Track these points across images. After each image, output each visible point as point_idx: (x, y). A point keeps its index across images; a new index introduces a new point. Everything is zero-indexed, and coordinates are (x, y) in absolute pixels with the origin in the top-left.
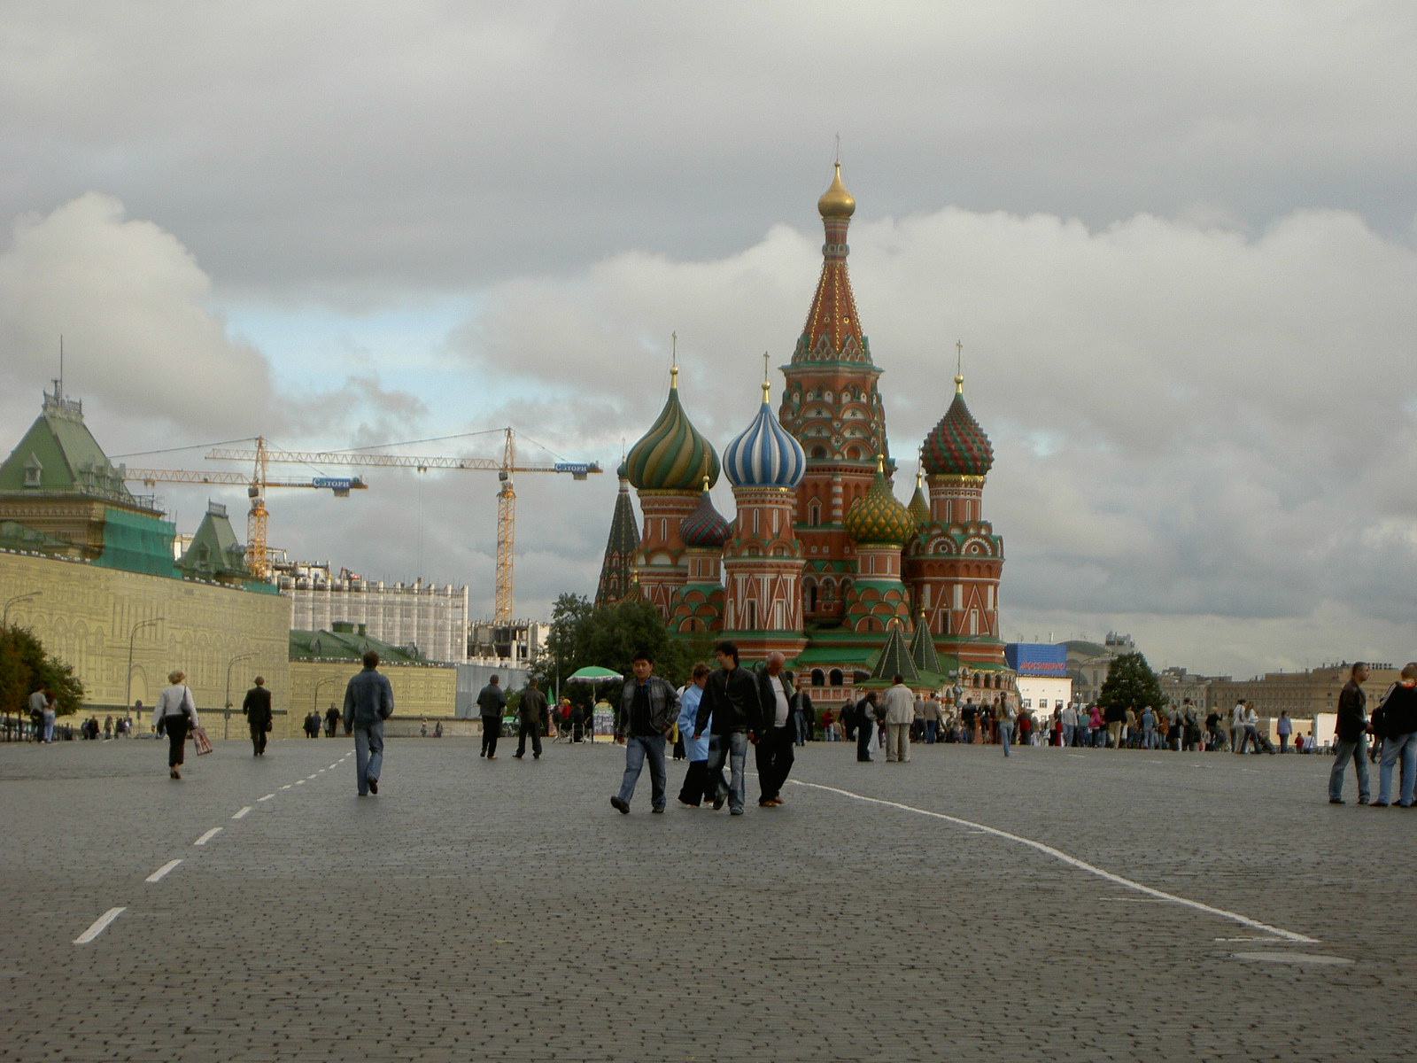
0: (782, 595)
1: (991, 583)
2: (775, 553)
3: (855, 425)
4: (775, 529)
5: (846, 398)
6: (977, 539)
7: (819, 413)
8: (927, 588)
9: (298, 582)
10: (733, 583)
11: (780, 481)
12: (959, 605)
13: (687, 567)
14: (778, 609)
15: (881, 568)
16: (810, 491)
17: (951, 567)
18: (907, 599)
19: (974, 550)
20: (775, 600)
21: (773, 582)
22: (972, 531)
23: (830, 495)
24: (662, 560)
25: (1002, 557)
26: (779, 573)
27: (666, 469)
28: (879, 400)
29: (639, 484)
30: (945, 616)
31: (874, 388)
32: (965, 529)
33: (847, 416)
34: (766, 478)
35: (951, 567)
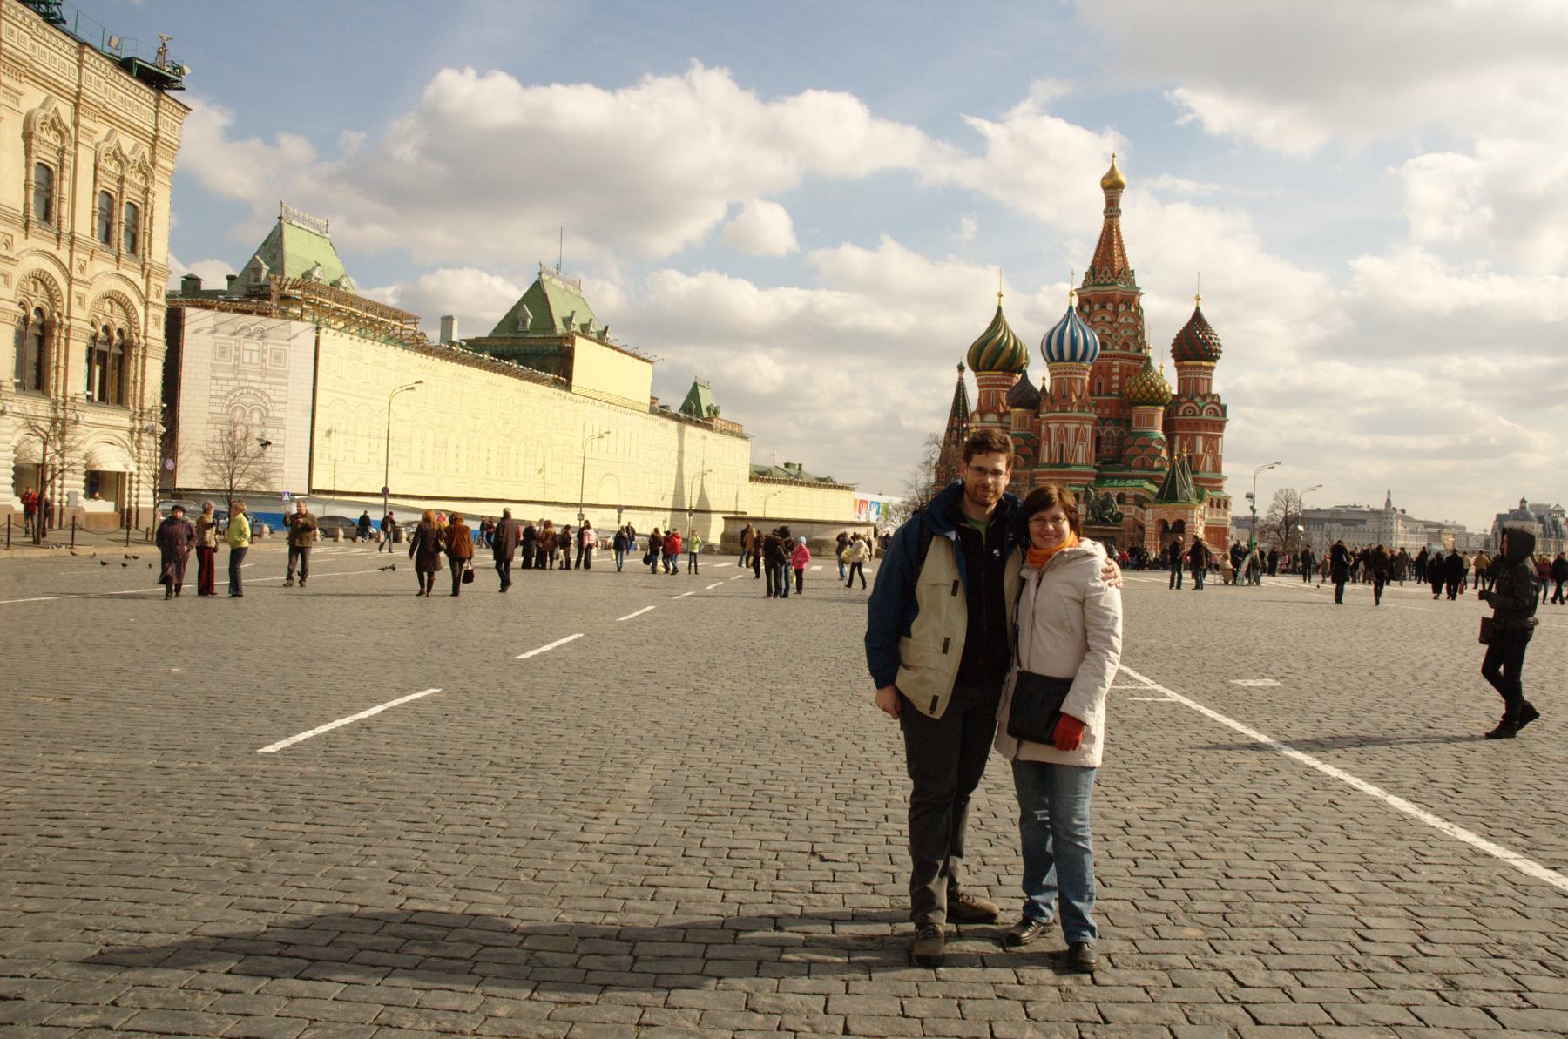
3: (1128, 325)
5: (1122, 308)
8: (1178, 439)
9: (673, 274)
10: (1049, 430)
11: (1083, 359)
12: (1200, 450)
14: (1080, 449)
17: (1197, 425)
21: (1077, 430)
23: (1110, 374)
27: (994, 355)
29: (976, 368)
33: (1122, 320)
34: (1073, 358)
35: (1197, 425)
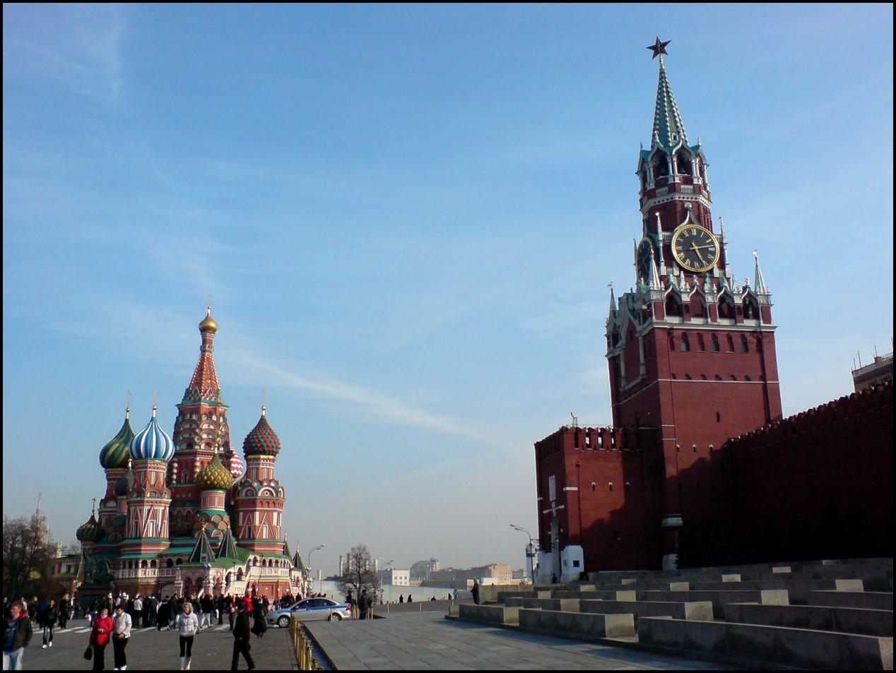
0: (155, 517)
1: (275, 511)
2: (150, 495)
4: (152, 483)
5: (204, 418)
6: (267, 488)
7: (191, 426)
8: (241, 514)
15: (212, 503)
16: (183, 465)
18: (227, 518)
19: (267, 493)
20: (149, 520)
21: (149, 510)
22: (265, 484)
25: (284, 498)
26: (152, 506)
28: (225, 420)
30: (250, 528)
31: (223, 415)
32: (261, 483)
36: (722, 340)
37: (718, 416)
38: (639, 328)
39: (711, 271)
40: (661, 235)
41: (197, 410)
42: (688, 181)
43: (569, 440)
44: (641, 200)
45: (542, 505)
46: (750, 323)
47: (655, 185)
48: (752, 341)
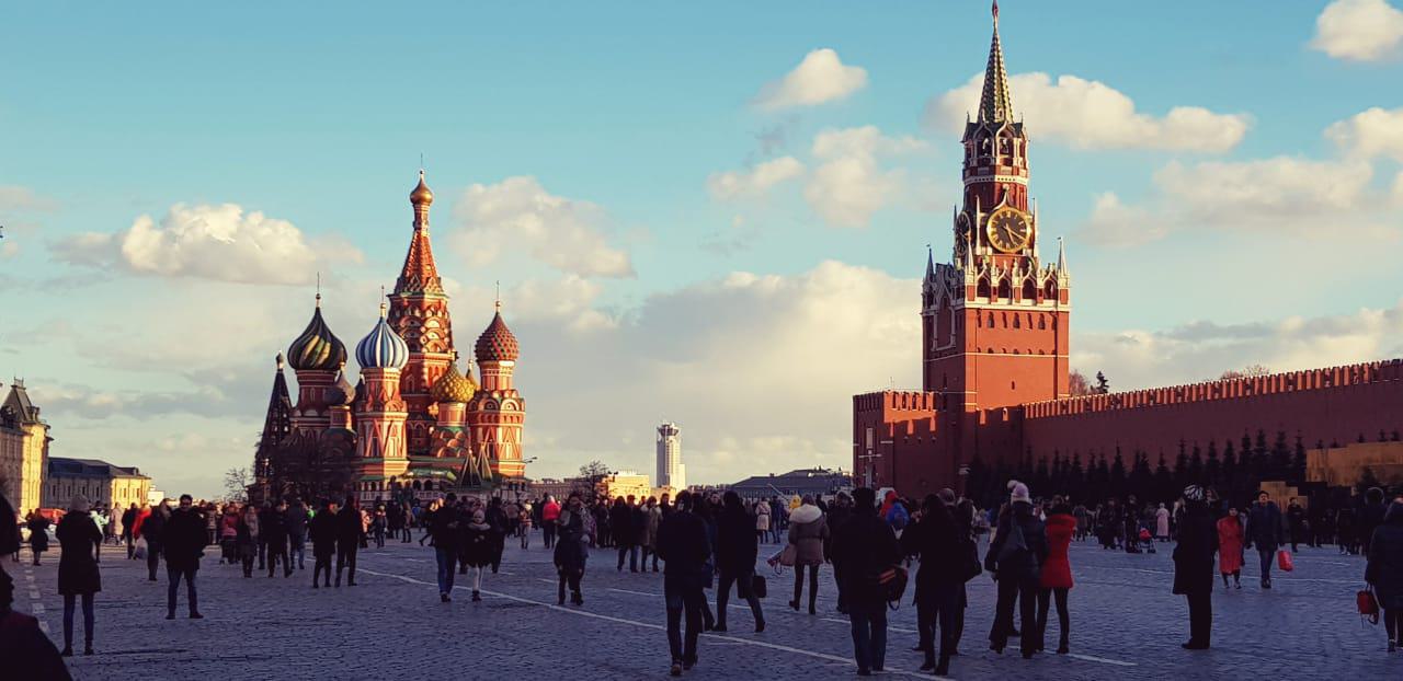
4: (390, 394)
5: (429, 314)
13: (329, 417)
22: (506, 395)
24: (312, 413)
29: (294, 364)
32: (502, 393)
36: (1023, 320)
37: (1013, 388)
38: (953, 303)
39: (1020, 252)
40: (980, 215)
41: (417, 302)
42: (1008, 162)
43: (888, 401)
44: (964, 171)
45: (857, 451)
46: (1047, 305)
47: (978, 162)
48: (1049, 320)
